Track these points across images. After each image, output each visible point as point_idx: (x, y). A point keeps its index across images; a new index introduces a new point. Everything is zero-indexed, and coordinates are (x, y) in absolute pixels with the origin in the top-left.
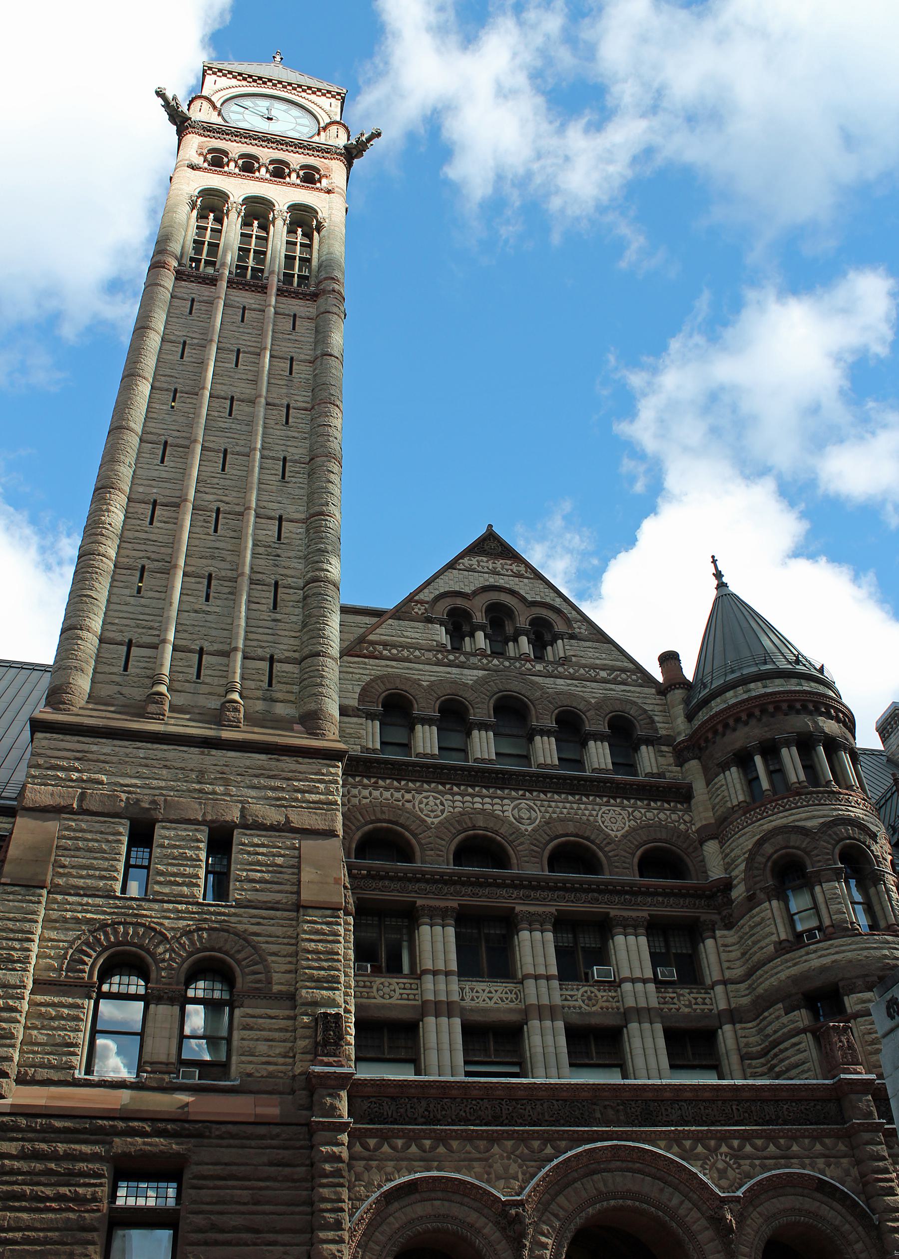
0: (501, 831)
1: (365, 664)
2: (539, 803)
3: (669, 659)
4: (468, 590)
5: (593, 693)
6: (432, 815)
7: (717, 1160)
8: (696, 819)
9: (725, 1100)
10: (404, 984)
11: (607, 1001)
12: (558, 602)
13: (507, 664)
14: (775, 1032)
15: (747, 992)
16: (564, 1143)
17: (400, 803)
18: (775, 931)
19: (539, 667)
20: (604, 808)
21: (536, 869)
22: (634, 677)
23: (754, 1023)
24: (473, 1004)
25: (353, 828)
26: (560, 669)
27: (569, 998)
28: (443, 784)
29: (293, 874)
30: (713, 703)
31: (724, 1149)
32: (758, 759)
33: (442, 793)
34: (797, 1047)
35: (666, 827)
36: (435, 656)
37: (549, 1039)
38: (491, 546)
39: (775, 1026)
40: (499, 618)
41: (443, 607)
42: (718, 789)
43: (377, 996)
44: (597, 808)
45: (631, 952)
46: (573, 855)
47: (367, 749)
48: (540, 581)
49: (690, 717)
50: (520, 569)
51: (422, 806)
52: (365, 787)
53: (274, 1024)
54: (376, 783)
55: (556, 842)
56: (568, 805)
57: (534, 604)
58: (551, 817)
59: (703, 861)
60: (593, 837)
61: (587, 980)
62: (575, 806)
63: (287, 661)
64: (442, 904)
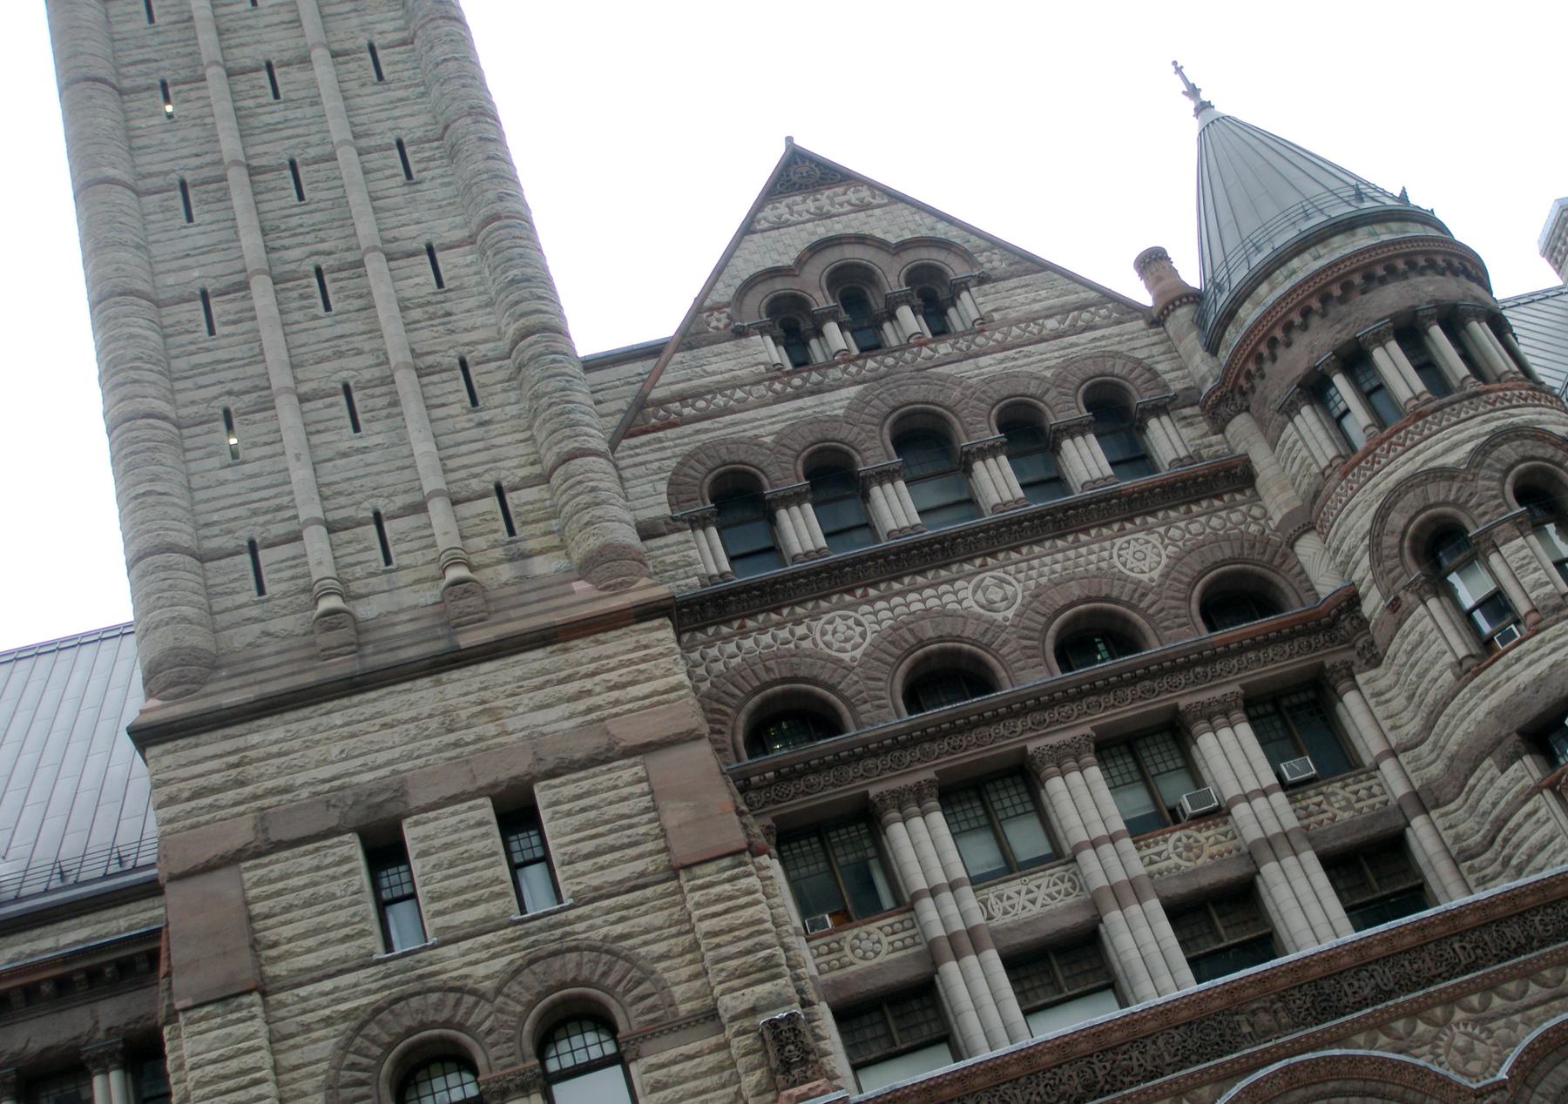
0: (966, 634)
1: (660, 440)
2: (1012, 568)
3: (1153, 263)
4: (787, 260)
6: (848, 646)
7: (1453, 1039)
8: (1271, 508)
9: (1439, 940)
10: (891, 926)
11: (1217, 842)
12: (942, 230)
13: (890, 361)
14: (1494, 804)
15: (1433, 756)
16: (1207, 1089)
17: (792, 646)
18: (1445, 647)
19: (944, 348)
20: (1119, 542)
22: (1103, 312)
23: (1459, 801)
24: (1008, 919)
25: (729, 711)
26: (980, 340)
27: (1156, 858)
28: (850, 591)
29: (651, 821)
30: (1242, 312)
31: (1459, 1015)
32: (1339, 381)
33: (853, 606)
34: (1535, 818)
35: (1227, 538)
36: (769, 388)
37: (1145, 933)
38: (801, 174)
39: (1490, 797)
40: (855, 294)
42: (1291, 449)
43: (856, 960)
44: (1107, 544)
45: (1232, 756)
46: (1092, 634)
47: (711, 577)
48: (901, 205)
49: (1212, 348)
50: (861, 195)
51: (828, 638)
52: (727, 639)
53: (699, 1065)
54: (742, 626)
55: (1058, 621)
56: (1059, 556)
57: (903, 246)
58: (1038, 585)
59: (1302, 571)
60: (1115, 594)
61: (1176, 820)
62: (1071, 553)
64: (910, 781)
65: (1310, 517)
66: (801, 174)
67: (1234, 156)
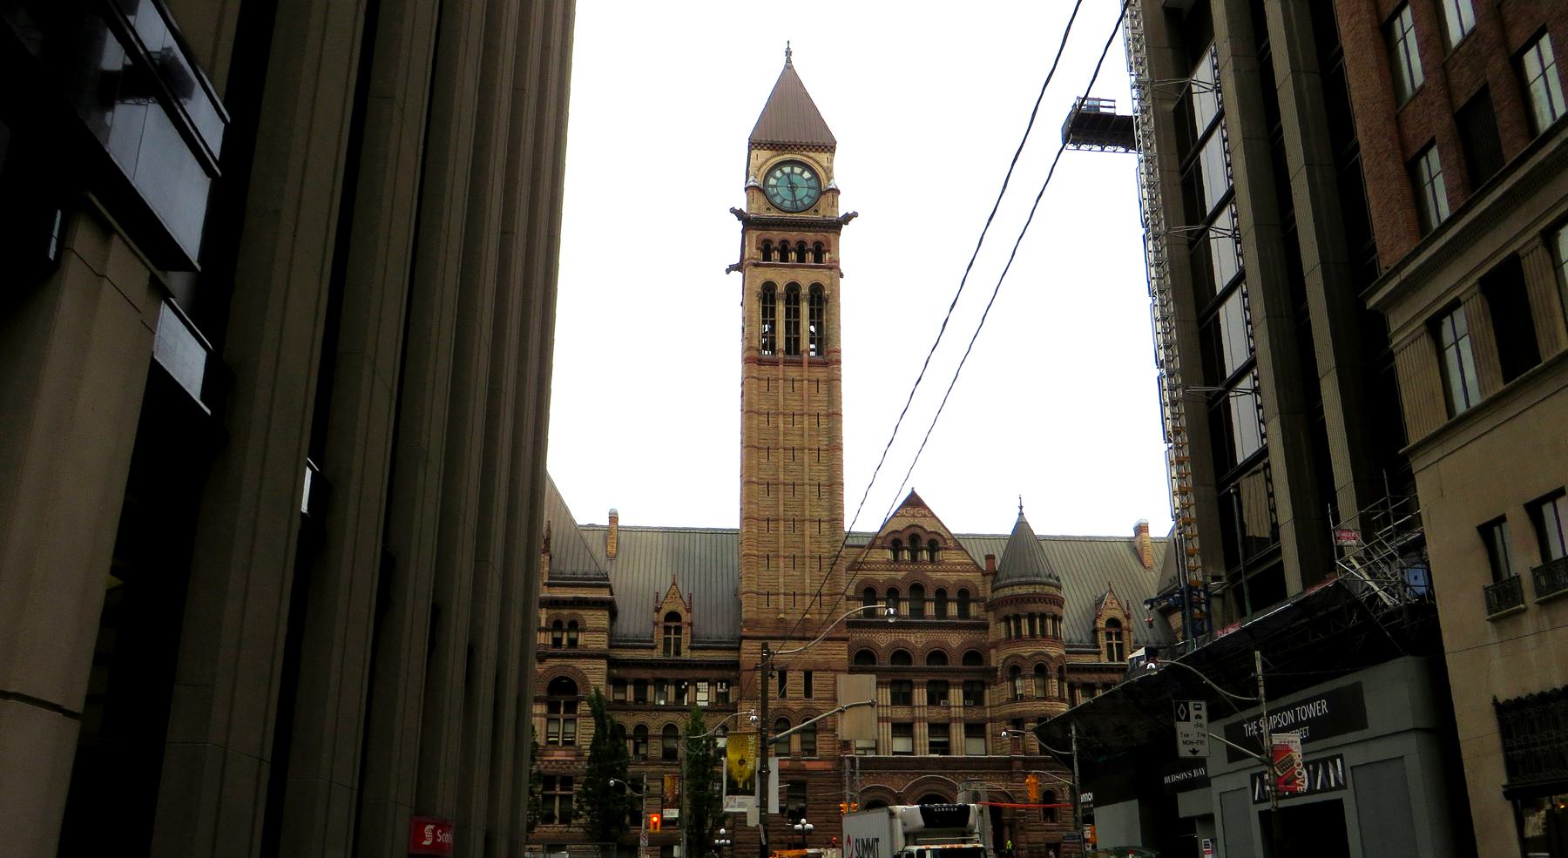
5: (953, 577)
21: (922, 664)
38: (913, 501)
41: (891, 538)
45: (956, 696)
46: (938, 656)
49: (994, 590)
65: (995, 645)
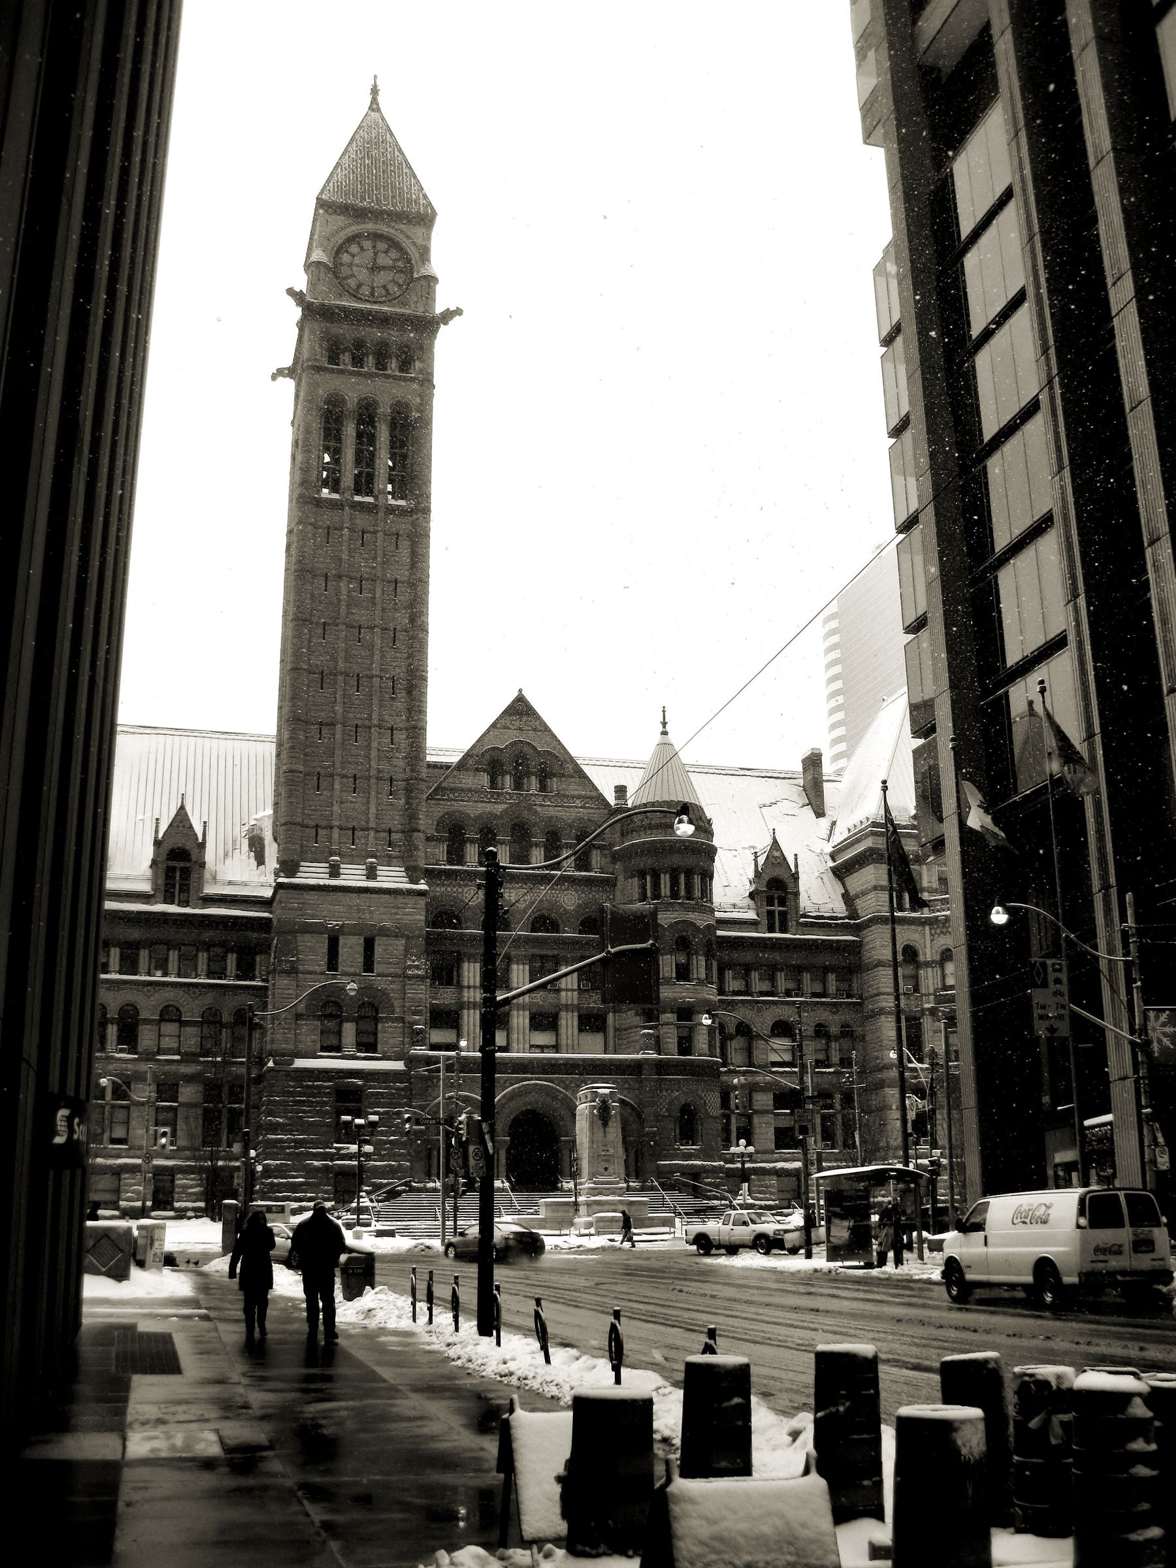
3: (621, 791)
37: (521, 1019)
38: (520, 709)
63: (397, 832)
66: (520, 709)
67: (666, 758)
